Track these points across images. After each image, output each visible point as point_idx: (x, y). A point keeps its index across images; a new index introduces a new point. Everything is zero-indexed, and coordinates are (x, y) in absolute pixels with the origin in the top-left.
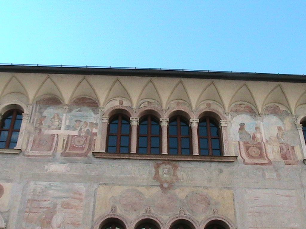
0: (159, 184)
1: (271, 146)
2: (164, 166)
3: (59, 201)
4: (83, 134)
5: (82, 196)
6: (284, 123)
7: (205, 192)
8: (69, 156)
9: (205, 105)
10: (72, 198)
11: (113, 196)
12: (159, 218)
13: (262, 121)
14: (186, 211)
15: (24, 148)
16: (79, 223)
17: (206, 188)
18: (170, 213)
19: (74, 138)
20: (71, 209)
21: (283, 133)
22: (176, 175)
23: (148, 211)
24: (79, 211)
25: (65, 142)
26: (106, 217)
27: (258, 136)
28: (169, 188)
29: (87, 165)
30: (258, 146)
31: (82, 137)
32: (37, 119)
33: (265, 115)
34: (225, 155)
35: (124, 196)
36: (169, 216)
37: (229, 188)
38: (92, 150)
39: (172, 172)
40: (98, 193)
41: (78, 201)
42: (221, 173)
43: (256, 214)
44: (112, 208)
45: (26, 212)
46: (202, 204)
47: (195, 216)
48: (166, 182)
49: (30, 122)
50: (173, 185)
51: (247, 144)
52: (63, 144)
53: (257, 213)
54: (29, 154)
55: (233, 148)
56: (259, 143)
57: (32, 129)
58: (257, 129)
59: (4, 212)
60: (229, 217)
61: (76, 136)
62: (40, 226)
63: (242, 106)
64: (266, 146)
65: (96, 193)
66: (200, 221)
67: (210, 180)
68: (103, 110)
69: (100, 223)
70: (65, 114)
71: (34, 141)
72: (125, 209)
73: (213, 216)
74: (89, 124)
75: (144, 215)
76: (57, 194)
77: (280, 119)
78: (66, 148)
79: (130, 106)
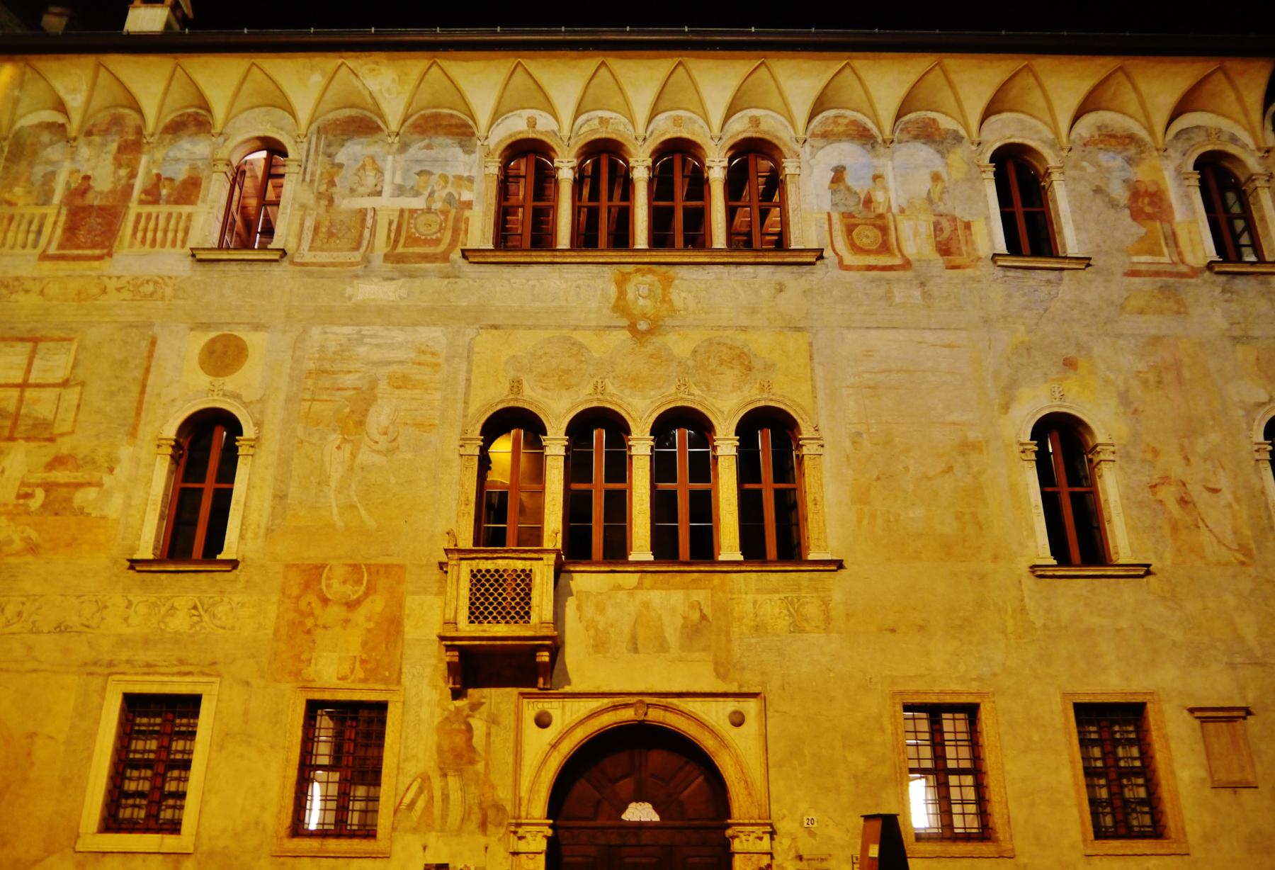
0: (625, 322)
1: (912, 222)
2: (638, 278)
3: (383, 372)
4: (437, 205)
6: (949, 162)
7: (740, 338)
8: (403, 262)
9: (746, 120)
10: (414, 363)
11: (514, 356)
12: (624, 407)
13: (892, 159)
14: (693, 386)
15: (291, 247)
17: (744, 329)
18: (652, 393)
19: (415, 215)
20: (411, 389)
21: (945, 187)
22: (667, 299)
23: (599, 387)
25: (394, 227)
27: (879, 196)
28: (651, 331)
29: (449, 283)
30: (879, 222)
31: (435, 213)
32: (322, 174)
33: (900, 142)
34: (792, 247)
35: (541, 353)
37: (798, 329)
38: (459, 244)
39: (660, 291)
40: (476, 350)
42: (781, 291)
43: (864, 390)
44: (513, 384)
45: (304, 400)
46: (732, 368)
48: (644, 316)
49: (304, 180)
50: (661, 323)
51: (848, 217)
52: (389, 230)
53: (869, 388)
54: (306, 259)
55: (814, 228)
56: (881, 216)
57: (308, 197)
58: (878, 180)
59: (251, 403)
60: (799, 400)
61: (419, 212)
62: (339, 432)
63: (840, 120)
64: (898, 222)
66: (726, 410)
67: (754, 311)
68: (486, 143)
70: (390, 158)
71: (316, 229)
72: (544, 385)
73: (759, 397)
74: (451, 179)
75: (592, 398)
76: (376, 355)
77: (938, 152)
78: (396, 242)
79: (553, 131)
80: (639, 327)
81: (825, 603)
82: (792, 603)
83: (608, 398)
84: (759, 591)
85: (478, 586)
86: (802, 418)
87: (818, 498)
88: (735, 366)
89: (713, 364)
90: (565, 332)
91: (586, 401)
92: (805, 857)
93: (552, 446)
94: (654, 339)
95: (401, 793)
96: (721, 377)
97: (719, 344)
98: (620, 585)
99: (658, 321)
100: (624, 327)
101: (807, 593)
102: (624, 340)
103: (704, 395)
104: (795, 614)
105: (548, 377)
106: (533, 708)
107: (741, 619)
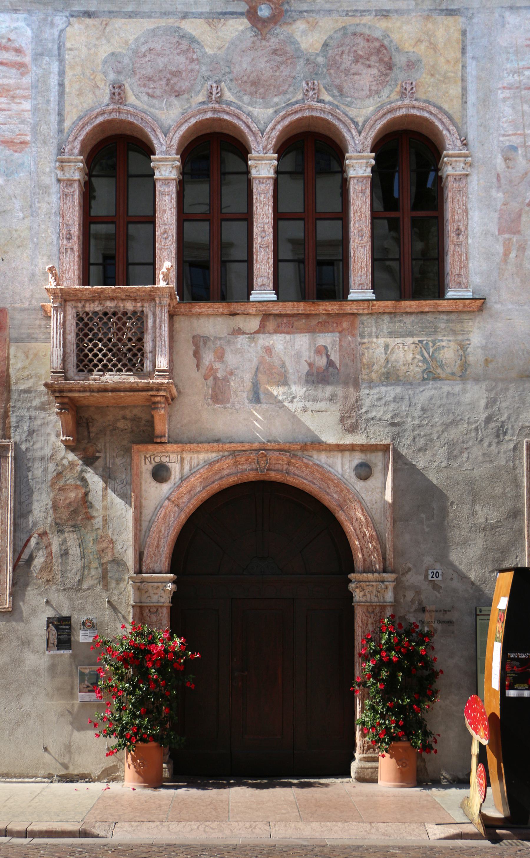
0: (243, 7)
5: (25, 55)
11: (113, 54)
12: (244, 118)
14: (323, 90)
16: (22, 138)
17: (385, 14)
18: (276, 100)
23: (214, 93)
24: (20, 103)
26: (96, 117)
35: (144, 49)
36: (275, 109)
37: (451, 13)
40: (68, 45)
41: (14, 71)
43: (523, 92)
46: (369, 66)
47: (347, 105)
50: (286, 7)
60: (446, 107)
65: (64, 44)
66: (360, 121)
69: (81, 138)
72: (150, 91)
73: (399, 103)
80: (259, 13)
81: (463, 347)
82: (426, 348)
83: (225, 107)
84: (392, 334)
85: (86, 331)
86: (448, 130)
87: (462, 228)
88: (372, 64)
89: (347, 61)
90: (171, 21)
91: (200, 112)
92: (428, 608)
93: (163, 169)
94: (278, 30)
95: (20, 549)
96: (356, 77)
97: (354, 34)
98: (240, 329)
99: (282, 4)
100: (242, 14)
101: (444, 336)
102: (242, 32)
103: (336, 103)
104: (429, 360)
105: (154, 81)
106: (150, 462)
107: (370, 365)
